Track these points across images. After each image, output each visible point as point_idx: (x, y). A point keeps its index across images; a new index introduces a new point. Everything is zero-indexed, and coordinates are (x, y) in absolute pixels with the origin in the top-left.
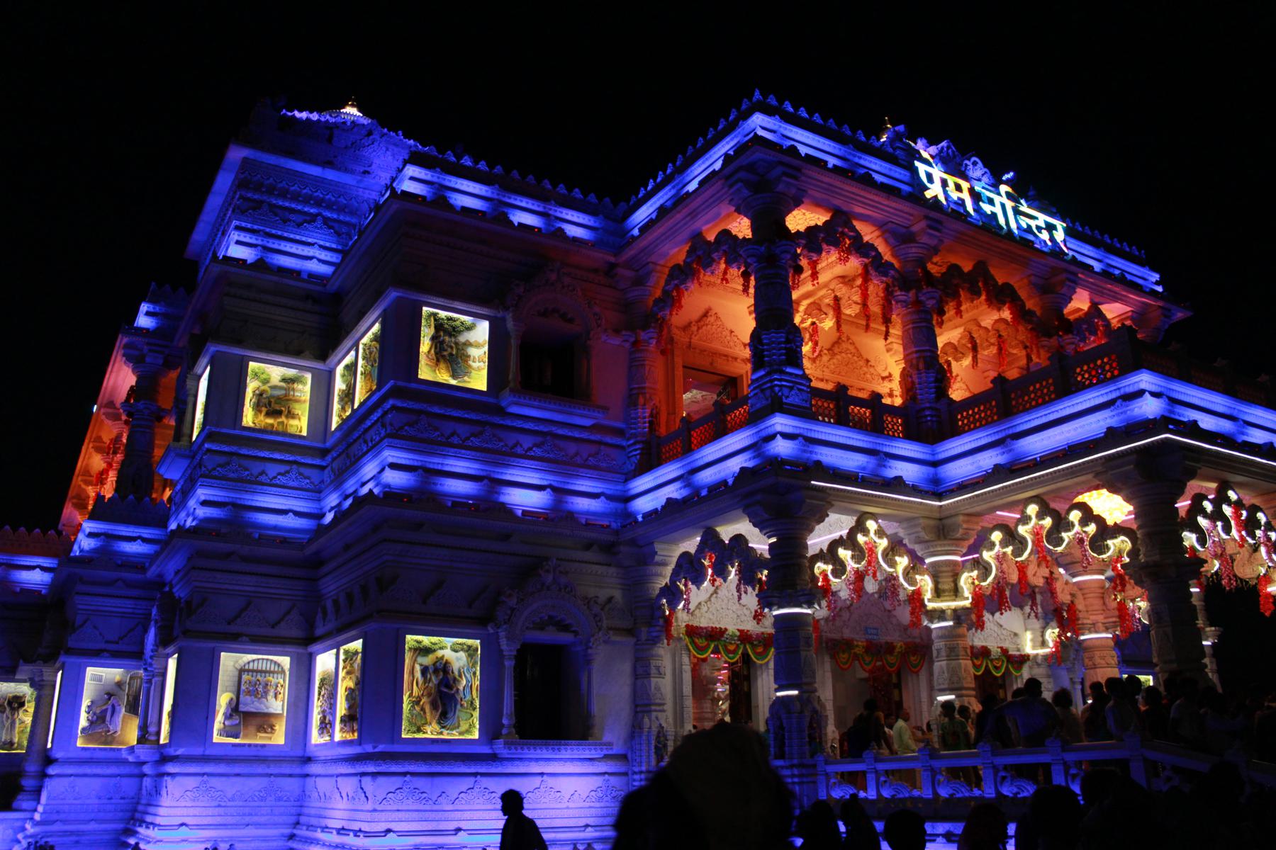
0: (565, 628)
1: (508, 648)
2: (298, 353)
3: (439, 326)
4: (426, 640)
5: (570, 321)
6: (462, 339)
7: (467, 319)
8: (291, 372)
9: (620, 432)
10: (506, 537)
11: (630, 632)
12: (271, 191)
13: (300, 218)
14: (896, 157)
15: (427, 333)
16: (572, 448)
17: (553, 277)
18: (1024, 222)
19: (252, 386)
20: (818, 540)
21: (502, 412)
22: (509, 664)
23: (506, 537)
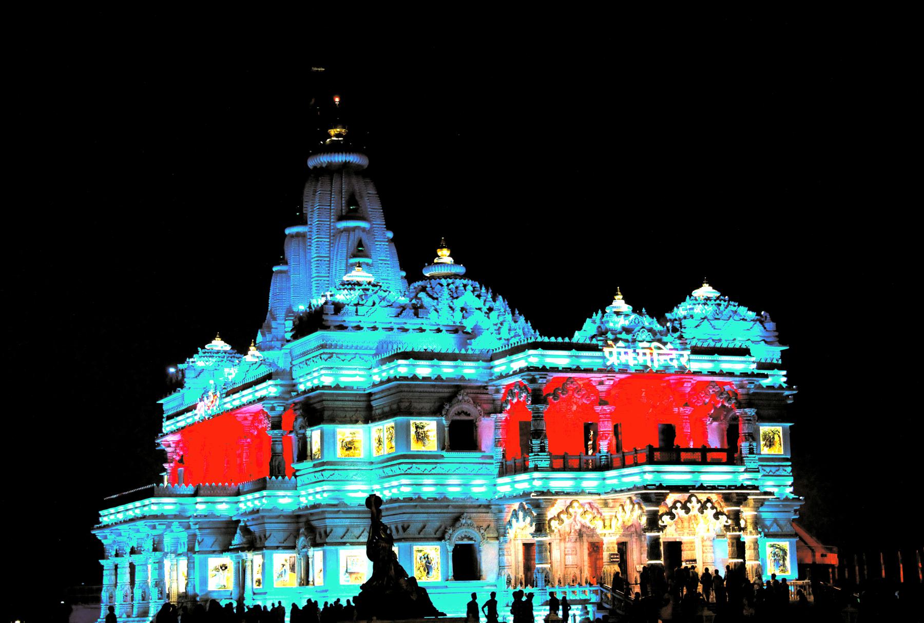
0: (471, 539)
1: (451, 549)
2: (356, 422)
3: (417, 427)
4: (420, 548)
5: (469, 415)
6: (425, 429)
7: (428, 422)
8: (353, 431)
9: (492, 457)
10: (447, 507)
11: (497, 538)
12: (336, 347)
13: (349, 357)
14: (597, 345)
15: (413, 430)
16: (470, 467)
17: (460, 398)
18: (662, 358)
19: (339, 438)
20: (551, 513)
21: (442, 457)
22: (451, 554)
23: (447, 507)
